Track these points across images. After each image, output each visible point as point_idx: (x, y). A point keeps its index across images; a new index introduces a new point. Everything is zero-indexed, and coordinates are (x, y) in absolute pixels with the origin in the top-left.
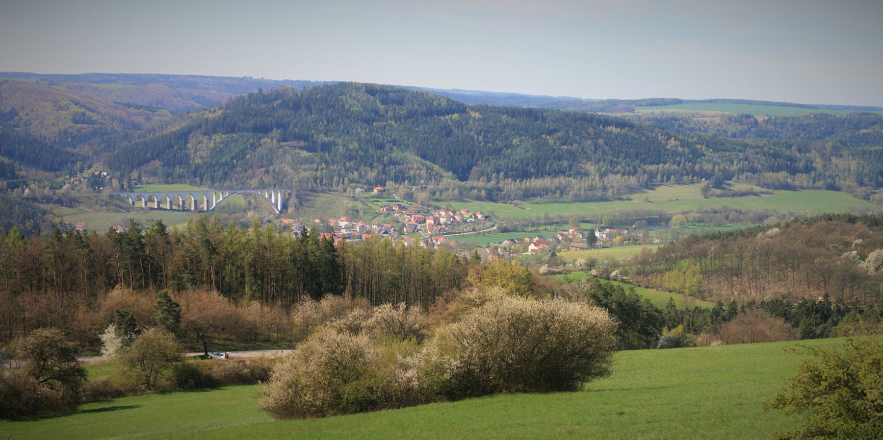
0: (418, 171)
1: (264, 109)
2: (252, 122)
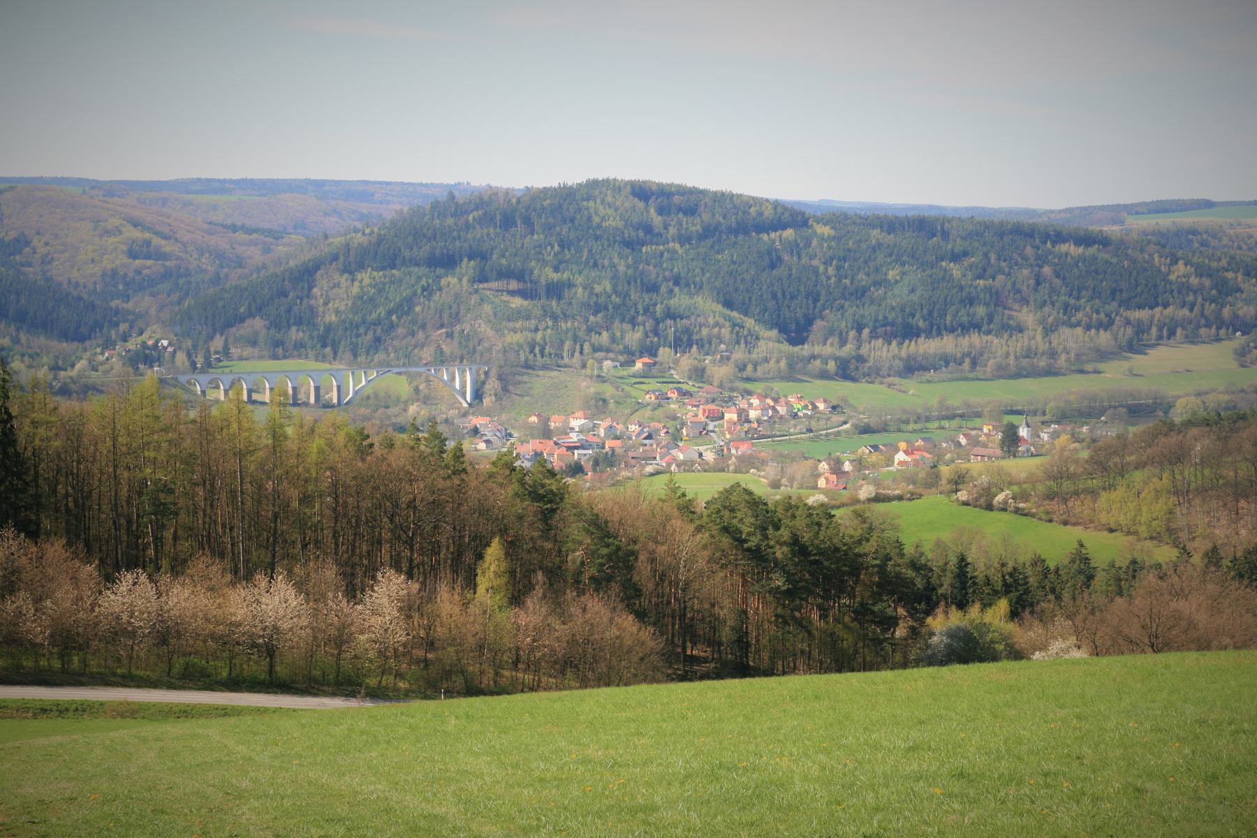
0: (716, 330)
1: (449, 227)
2: (426, 248)
